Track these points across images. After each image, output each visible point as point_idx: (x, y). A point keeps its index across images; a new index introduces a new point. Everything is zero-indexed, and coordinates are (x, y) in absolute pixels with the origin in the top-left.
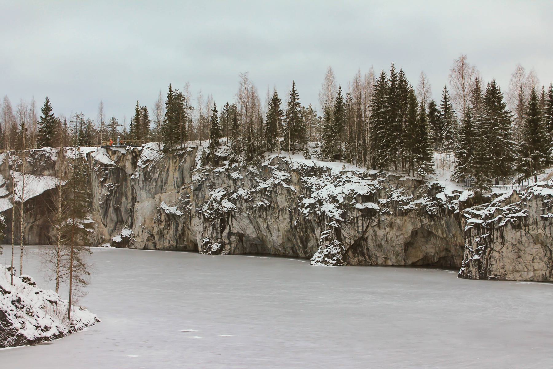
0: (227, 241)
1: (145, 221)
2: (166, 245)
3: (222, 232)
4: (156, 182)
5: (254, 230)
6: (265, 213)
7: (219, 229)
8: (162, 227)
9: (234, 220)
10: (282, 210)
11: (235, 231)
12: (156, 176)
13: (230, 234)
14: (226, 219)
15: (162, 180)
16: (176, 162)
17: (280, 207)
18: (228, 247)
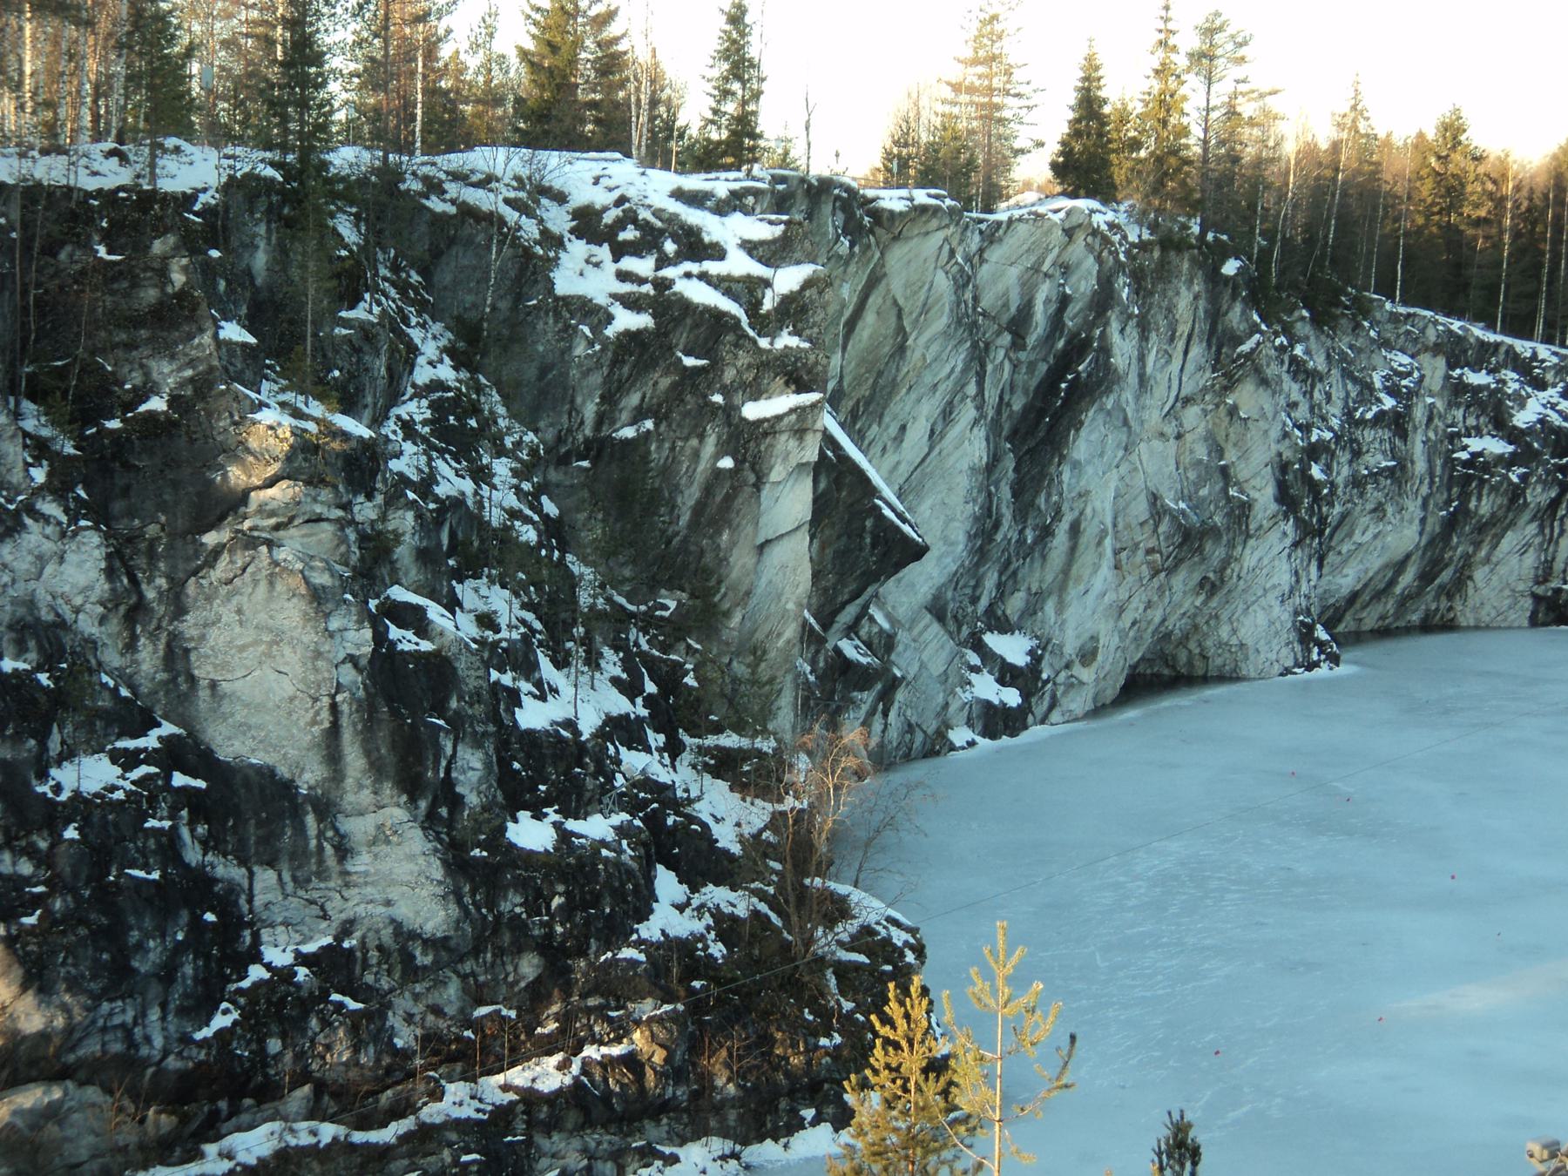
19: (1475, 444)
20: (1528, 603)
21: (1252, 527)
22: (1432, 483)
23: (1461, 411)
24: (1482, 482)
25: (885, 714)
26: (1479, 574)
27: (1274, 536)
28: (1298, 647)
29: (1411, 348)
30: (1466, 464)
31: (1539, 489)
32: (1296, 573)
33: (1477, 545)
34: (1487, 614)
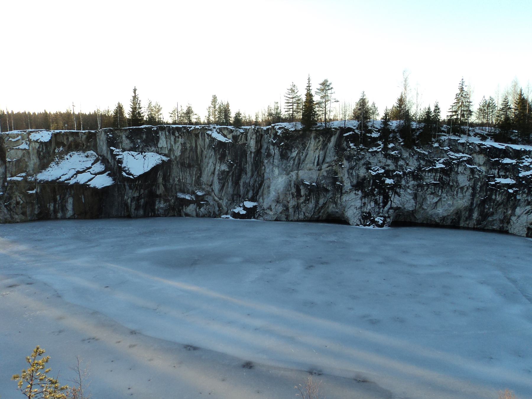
0: (387, 215)
1: (279, 196)
2: (301, 217)
3: (384, 207)
4: (294, 160)
5: (414, 204)
6: (440, 191)
7: (381, 204)
8: (302, 200)
9: (396, 196)
10: (462, 188)
11: (394, 205)
12: (294, 154)
13: (391, 208)
14: (390, 196)
15: (299, 159)
16: (319, 141)
17: (461, 186)
18: (388, 220)
19: (498, 180)
20: (525, 229)
21: (343, 191)
22: (474, 188)
23: (497, 171)
24: (497, 191)
25: (200, 208)
26: (514, 219)
27: (352, 195)
28: (362, 221)
29: (470, 152)
30: (493, 185)
31: (525, 196)
32: (365, 204)
33: (507, 209)
34: (515, 231)
